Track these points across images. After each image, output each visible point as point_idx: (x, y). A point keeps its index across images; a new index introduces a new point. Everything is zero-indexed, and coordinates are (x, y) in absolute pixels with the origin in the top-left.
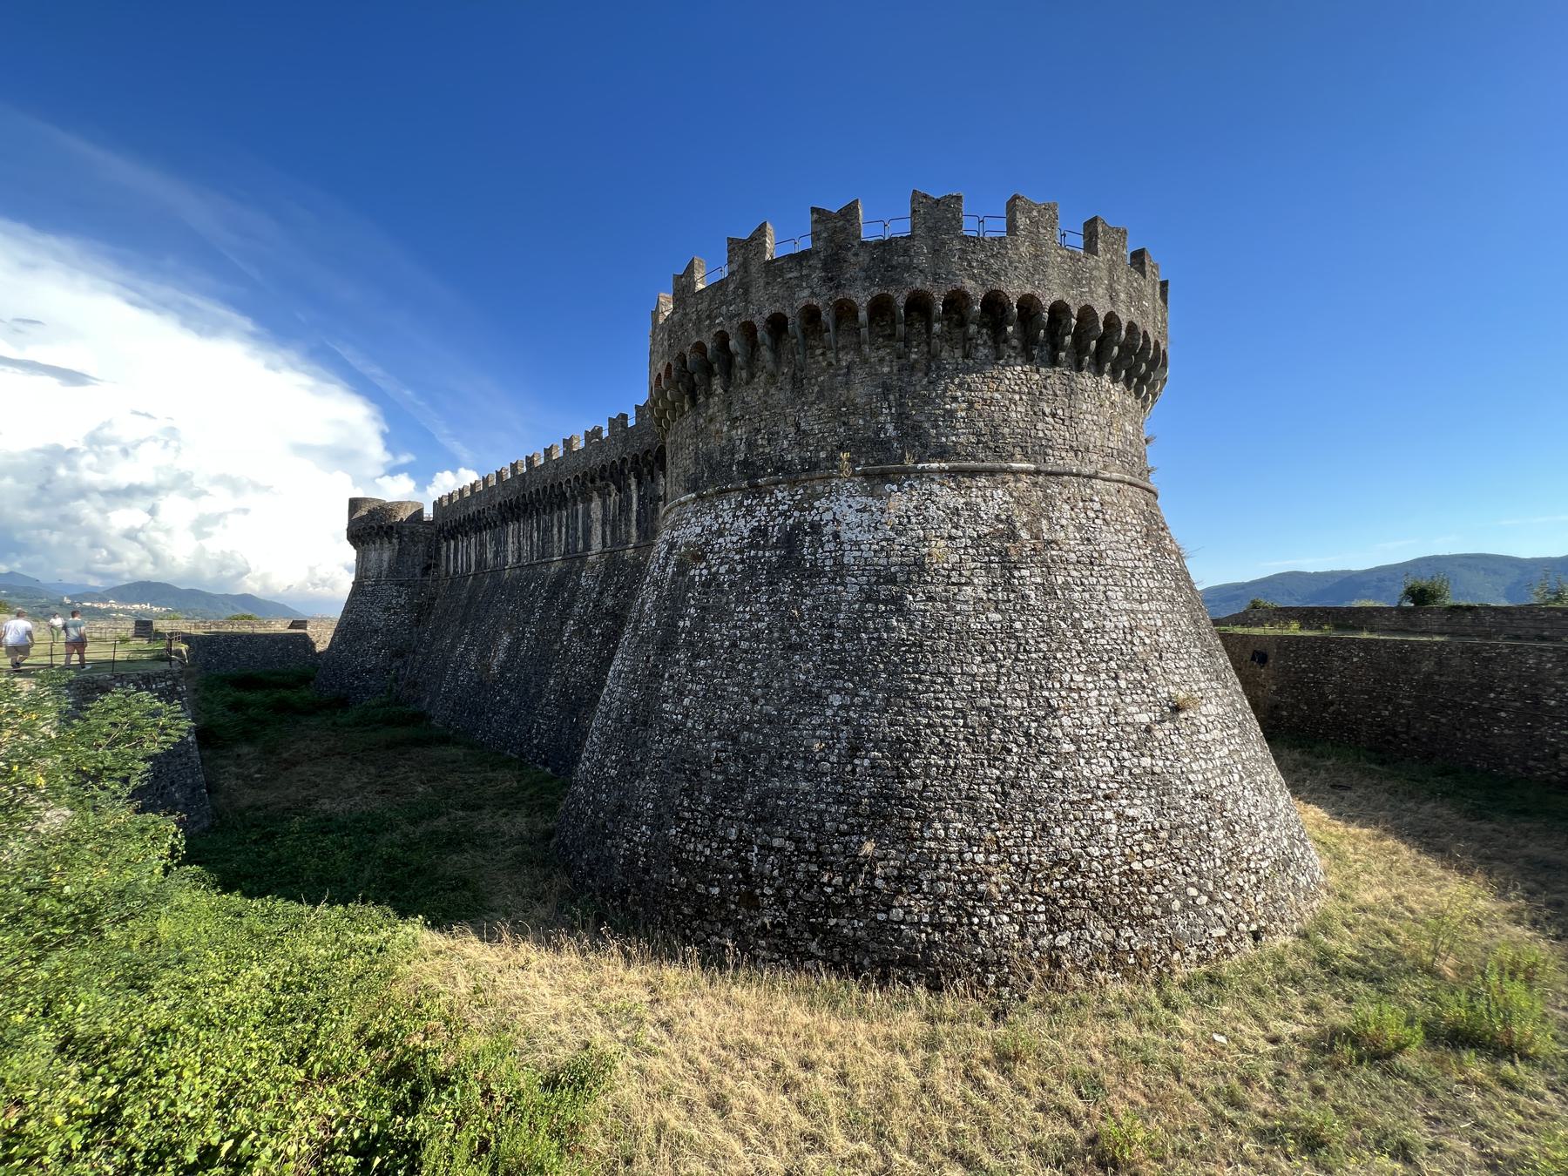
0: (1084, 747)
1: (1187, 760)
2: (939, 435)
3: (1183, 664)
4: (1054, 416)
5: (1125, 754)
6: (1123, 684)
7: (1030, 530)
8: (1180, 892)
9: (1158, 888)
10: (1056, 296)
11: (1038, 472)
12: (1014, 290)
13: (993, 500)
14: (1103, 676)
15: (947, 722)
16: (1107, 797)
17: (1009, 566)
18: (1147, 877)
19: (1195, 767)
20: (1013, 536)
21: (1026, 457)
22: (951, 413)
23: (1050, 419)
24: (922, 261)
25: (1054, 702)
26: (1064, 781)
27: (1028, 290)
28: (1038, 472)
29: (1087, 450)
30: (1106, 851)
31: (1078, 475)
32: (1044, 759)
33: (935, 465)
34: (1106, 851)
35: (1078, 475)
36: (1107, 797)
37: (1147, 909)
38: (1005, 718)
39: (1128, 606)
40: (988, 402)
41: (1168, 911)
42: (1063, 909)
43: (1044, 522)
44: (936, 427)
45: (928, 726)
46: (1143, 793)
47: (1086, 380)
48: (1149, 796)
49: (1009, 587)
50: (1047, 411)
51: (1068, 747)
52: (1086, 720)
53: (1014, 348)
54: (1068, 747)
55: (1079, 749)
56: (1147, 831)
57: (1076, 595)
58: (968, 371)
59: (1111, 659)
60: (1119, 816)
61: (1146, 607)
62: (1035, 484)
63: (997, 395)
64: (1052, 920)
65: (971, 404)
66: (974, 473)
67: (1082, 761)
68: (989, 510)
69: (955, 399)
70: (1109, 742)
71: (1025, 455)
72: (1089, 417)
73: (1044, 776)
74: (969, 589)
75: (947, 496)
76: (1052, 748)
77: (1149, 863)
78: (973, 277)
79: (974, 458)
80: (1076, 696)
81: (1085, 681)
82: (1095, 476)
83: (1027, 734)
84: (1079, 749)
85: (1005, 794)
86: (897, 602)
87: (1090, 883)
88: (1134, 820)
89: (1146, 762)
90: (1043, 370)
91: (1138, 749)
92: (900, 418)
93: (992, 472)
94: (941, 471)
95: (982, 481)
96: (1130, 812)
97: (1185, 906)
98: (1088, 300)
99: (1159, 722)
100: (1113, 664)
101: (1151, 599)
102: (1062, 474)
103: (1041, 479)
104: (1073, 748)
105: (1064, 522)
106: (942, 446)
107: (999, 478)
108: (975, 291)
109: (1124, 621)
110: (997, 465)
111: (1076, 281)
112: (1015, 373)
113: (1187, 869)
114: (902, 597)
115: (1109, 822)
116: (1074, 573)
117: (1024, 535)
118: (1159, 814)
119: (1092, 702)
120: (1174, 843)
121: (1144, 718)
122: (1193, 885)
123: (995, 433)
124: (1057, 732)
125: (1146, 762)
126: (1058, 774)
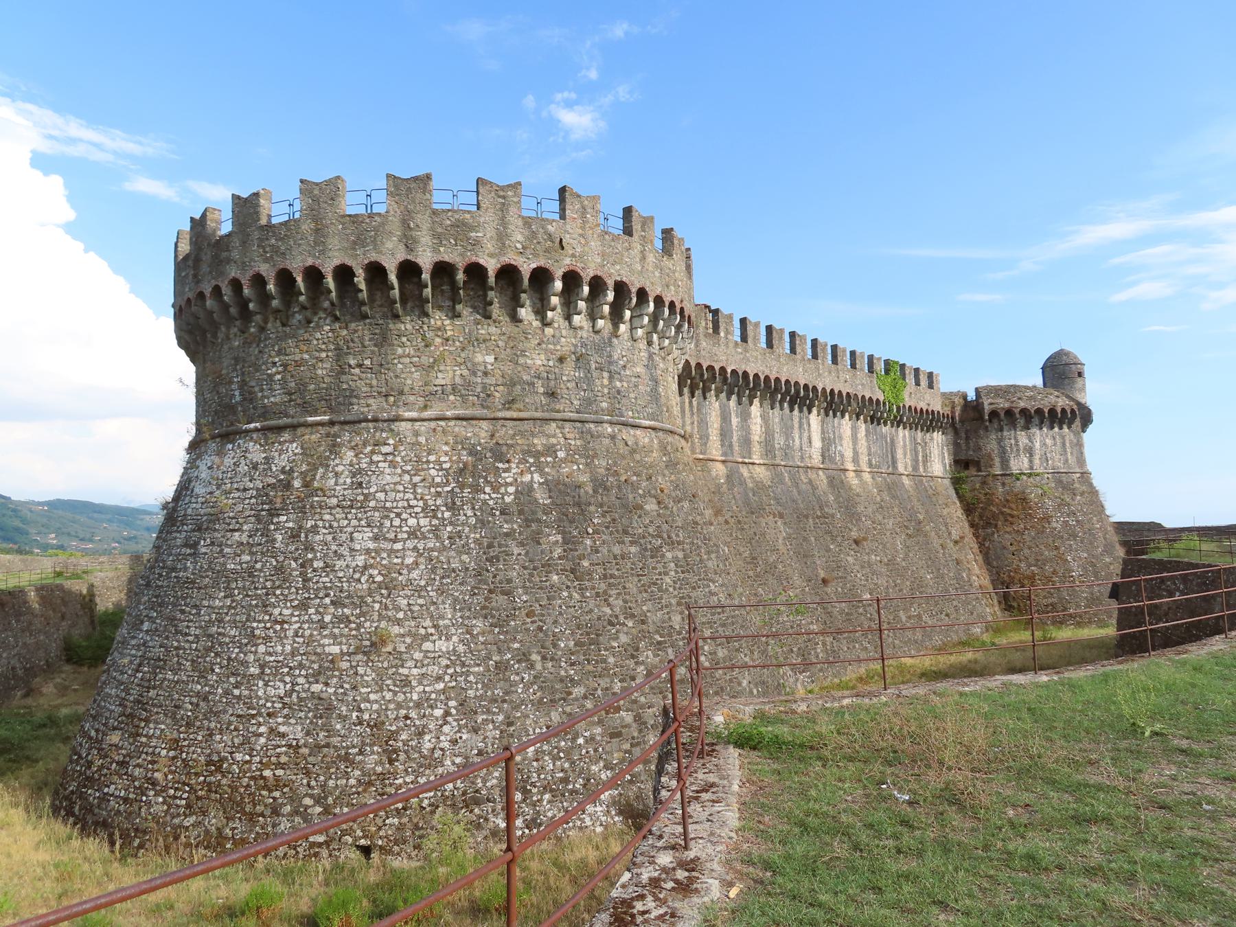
0: (268, 671)
1: (363, 690)
2: (264, 397)
3: (421, 601)
4: (360, 366)
5: (301, 680)
6: (327, 619)
7: (304, 479)
8: (294, 799)
9: (277, 794)
10: (337, 262)
11: (332, 423)
12: (297, 264)
13: (287, 453)
14: (312, 611)
15: (187, 646)
16: (269, 715)
17: (273, 513)
18: (271, 782)
19: (372, 697)
20: (288, 486)
21: (331, 409)
22: (271, 376)
23: (357, 371)
24: (235, 254)
25: (257, 632)
26: (239, 698)
27: (310, 262)
28: (332, 423)
29: (401, 393)
30: (247, 758)
31: (375, 420)
32: (232, 680)
33: (252, 426)
34: (247, 758)
35: (375, 420)
36: (269, 715)
37: (259, 809)
38: (220, 644)
39: (371, 545)
40: (298, 364)
41: (276, 812)
42: (199, 798)
43: (321, 470)
44: (262, 390)
45: (177, 648)
46: (302, 714)
47: (407, 325)
48: (306, 717)
49: (266, 533)
50: (352, 362)
51: (254, 670)
52: (279, 648)
53: (326, 310)
54: (254, 670)
55: (263, 673)
56: (290, 746)
57: (318, 538)
58: (286, 336)
59: (327, 595)
60: (272, 730)
61: (398, 546)
62: (328, 435)
63: (306, 356)
64: (188, 806)
65: (285, 366)
66: (280, 429)
67: (261, 683)
68: (281, 461)
69: (274, 364)
70: (291, 668)
71: (330, 408)
72: (407, 360)
73: (227, 693)
74: (237, 534)
75: (256, 453)
76: (241, 670)
77: (280, 772)
78: (266, 260)
79: (287, 416)
80: (278, 627)
81: (292, 615)
82: (397, 419)
83: (229, 659)
84: (263, 673)
85: (197, 705)
86: (195, 545)
87: (224, 781)
88: (283, 735)
89: (316, 688)
90: (353, 326)
91: (316, 677)
92: (243, 384)
93: (294, 427)
94: (256, 430)
95: (286, 436)
96: (282, 729)
97: (296, 812)
98: (374, 257)
99: (350, 654)
100: (327, 601)
101: (412, 534)
102: (360, 422)
103: (336, 428)
104: (257, 671)
105: (340, 468)
106: (265, 407)
107: (300, 431)
108: (267, 271)
109: (360, 560)
110: (295, 421)
111: (359, 242)
112: (325, 332)
113: (313, 783)
114: (199, 543)
115: (261, 735)
116: (327, 517)
117: (297, 484)
118: (308, 734)
119: (290, 633)
120: (310, 759)
121: (335, 649)
122: (311, 796)
123: (302, 387)
124: (251, 658)
125: (316, 688)
126: (236, 692)
